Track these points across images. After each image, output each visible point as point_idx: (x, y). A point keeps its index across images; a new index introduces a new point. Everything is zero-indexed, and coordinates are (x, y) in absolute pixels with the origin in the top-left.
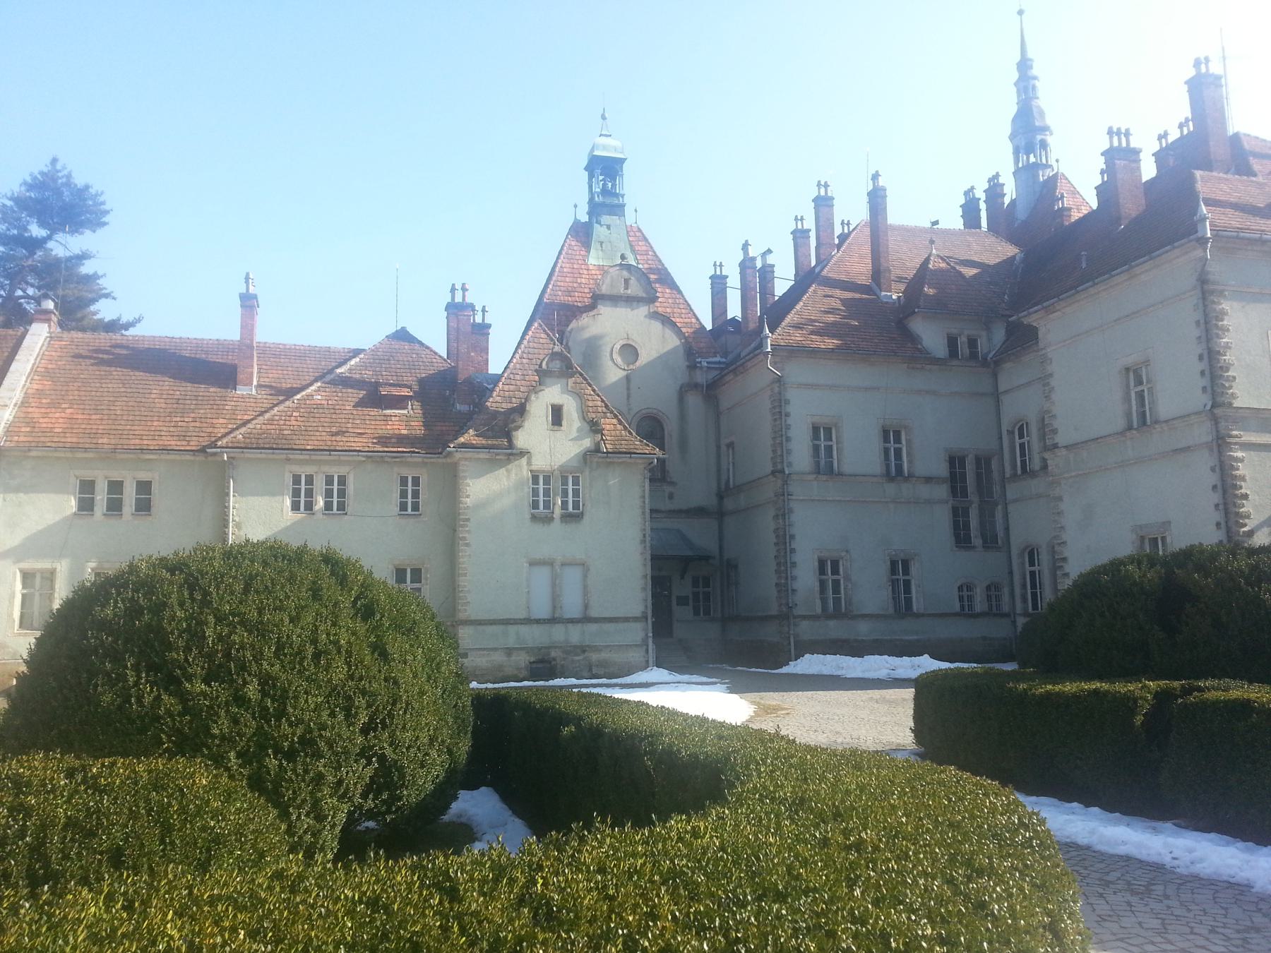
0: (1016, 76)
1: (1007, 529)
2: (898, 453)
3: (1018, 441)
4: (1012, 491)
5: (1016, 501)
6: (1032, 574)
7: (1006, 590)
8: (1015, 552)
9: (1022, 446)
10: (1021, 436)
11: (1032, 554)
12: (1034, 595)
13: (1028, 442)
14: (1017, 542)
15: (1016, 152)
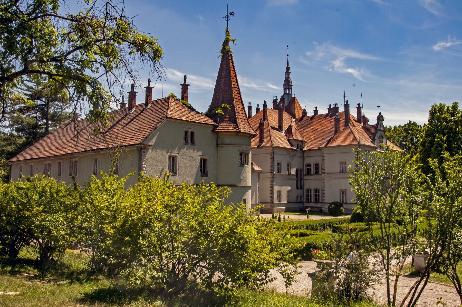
0: (286, 71)
1: (304, 185)
2: (289, 168)
3: (307, 167)
4: (305, 177)
5: (306, 179)
6: (308, 194)
7: (303, 197)
8: (305, 190)
9: (308, 169)
10: (308, 166)
11: (309, 190)
12: (308, 199)
13: (310, 168)
14: (306, 187)
15: (285, 89)
